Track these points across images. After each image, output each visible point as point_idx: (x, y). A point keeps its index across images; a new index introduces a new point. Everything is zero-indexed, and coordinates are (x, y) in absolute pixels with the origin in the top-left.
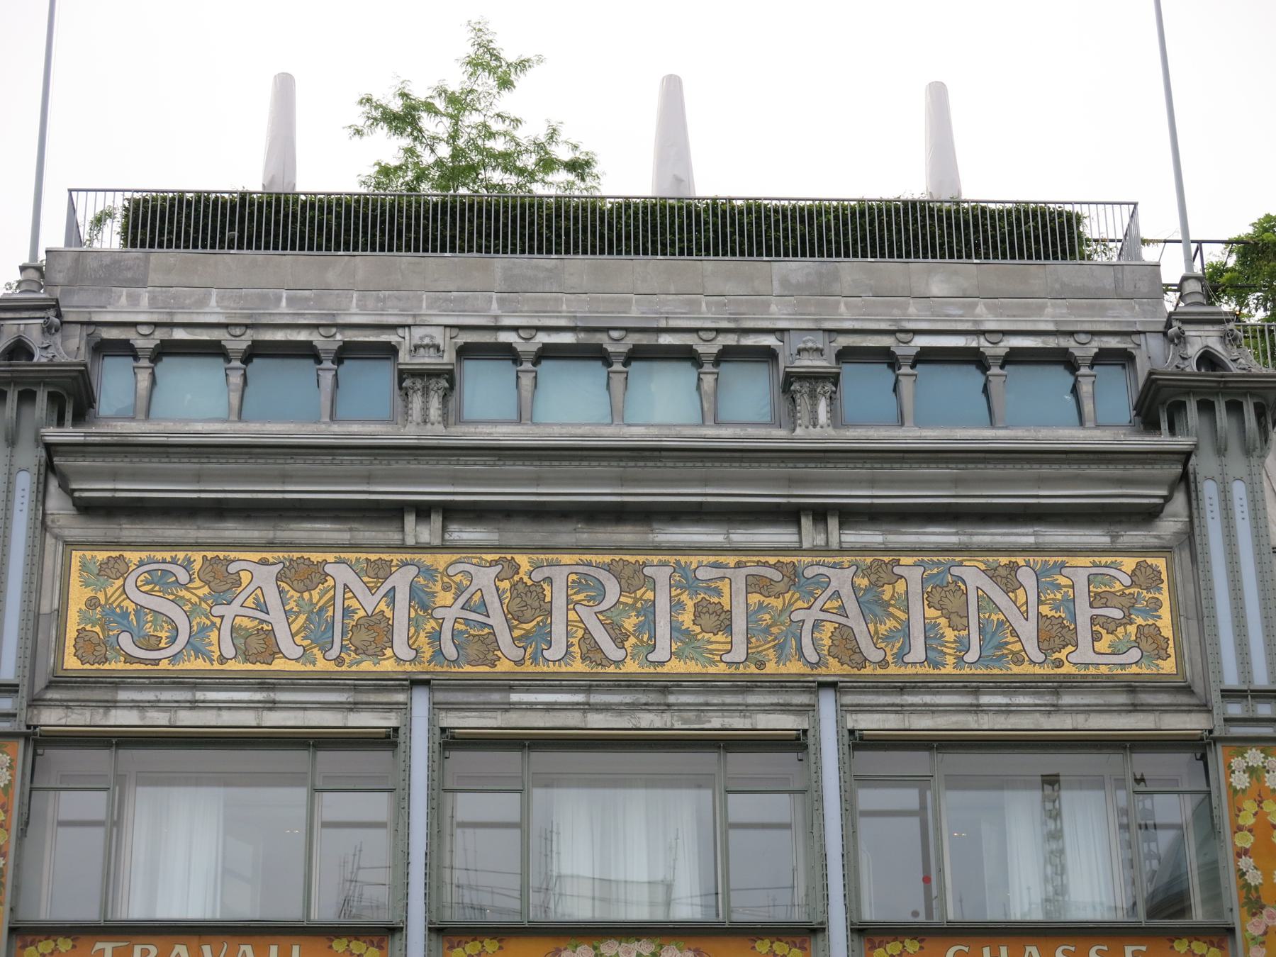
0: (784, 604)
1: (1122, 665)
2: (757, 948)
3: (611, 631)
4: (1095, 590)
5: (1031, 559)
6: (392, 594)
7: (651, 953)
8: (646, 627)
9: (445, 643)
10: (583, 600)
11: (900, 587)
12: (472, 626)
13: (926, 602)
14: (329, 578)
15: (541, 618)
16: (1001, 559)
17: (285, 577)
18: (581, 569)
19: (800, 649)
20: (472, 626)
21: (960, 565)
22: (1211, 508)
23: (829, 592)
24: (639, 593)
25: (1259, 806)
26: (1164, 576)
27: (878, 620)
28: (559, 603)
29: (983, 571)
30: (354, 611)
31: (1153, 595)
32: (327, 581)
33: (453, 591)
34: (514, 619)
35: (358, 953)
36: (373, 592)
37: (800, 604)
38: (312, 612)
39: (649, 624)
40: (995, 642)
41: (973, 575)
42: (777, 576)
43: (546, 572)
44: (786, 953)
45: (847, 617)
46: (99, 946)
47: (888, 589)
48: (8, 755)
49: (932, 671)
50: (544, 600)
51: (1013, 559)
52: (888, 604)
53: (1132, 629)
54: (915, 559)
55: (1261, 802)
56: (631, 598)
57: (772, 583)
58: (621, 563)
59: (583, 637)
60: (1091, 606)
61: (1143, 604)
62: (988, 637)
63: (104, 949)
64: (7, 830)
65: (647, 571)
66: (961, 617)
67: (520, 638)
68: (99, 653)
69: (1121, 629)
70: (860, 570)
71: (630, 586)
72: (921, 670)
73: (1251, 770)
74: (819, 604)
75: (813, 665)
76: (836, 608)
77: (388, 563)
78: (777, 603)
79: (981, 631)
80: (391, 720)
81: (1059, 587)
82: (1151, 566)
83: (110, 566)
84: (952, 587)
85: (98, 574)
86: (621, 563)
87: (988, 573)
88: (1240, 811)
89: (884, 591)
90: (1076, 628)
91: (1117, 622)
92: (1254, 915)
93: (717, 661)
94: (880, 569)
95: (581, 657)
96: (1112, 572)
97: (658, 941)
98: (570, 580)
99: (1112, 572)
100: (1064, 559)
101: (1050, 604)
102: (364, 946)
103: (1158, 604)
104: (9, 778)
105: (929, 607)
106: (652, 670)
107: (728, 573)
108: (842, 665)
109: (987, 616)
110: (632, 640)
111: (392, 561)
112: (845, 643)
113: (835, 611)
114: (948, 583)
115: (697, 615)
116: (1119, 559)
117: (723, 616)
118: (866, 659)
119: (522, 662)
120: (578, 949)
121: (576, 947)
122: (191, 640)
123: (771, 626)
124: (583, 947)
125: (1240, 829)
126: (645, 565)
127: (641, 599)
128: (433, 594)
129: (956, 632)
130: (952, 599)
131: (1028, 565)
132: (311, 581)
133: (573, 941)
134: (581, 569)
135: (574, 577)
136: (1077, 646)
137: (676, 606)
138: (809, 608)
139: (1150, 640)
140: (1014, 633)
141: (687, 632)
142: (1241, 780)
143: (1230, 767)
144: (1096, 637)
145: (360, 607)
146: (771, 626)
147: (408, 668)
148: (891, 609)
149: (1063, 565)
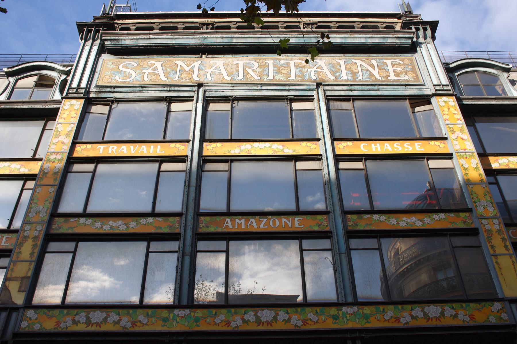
6: (194, 67)
25: (449, 109)
35: (178, 147)
41: (359, 62)
44: (311, 146)
55: (449, 109)
60: (393, 67)
65: (266, 61)
70: (326, 61)
73: (445, 102)
80: (191, 94)
88: (443, 110)
92: (453, 134)
102: (180, 146)
107: (289, 61)
117: (288, 70)
121: (246, 145)
122: (136, 77)
125: (444, 114)
139: (411, 75)
142: (442, 104)
143: (438, 101)
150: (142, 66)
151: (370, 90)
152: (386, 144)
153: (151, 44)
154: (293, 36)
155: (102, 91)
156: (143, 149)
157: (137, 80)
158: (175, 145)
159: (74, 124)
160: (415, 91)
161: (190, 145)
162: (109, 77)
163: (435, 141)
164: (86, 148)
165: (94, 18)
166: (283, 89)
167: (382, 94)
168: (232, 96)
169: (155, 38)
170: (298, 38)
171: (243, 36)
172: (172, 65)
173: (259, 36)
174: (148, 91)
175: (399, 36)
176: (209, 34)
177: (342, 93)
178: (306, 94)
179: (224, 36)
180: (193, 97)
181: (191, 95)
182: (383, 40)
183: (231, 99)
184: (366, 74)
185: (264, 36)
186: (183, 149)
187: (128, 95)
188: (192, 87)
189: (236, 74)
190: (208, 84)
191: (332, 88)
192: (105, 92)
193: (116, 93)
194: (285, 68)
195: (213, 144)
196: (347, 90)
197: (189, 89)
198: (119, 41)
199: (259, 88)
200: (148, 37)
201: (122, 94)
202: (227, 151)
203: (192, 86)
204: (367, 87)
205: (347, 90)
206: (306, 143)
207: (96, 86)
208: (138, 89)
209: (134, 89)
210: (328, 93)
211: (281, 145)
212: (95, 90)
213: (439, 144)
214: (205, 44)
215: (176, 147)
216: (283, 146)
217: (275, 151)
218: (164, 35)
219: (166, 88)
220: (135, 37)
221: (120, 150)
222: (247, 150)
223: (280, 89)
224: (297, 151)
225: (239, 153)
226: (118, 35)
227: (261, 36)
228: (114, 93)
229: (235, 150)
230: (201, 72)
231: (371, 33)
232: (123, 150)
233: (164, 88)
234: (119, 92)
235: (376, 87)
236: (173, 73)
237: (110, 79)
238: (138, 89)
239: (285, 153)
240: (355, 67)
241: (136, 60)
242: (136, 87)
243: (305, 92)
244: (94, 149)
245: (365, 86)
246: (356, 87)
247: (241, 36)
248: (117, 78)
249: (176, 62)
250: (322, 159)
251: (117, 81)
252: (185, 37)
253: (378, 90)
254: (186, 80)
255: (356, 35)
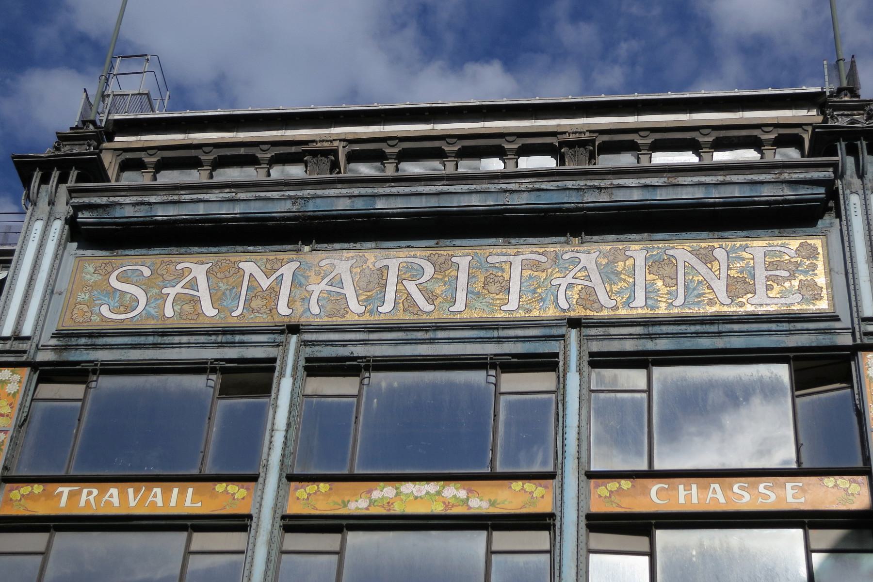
0: (547, 275)
1: (789, 305)
2: (513, 487)
3: (426, 295)
4: (769, 260)
5: (724, 244)
6: (281, 278)
7: (436, 492)
8: (450, 291)
9: (311, 307)
10: (408, 277)
11: (630, 262)
12: (332, 295)
13: (647, 271)
14: (240, 270)
15: (378, 288)
16: (701, 244)
17: (213, 271)
18: (409, 260)
19: (556, 303)
20: (332, 295)
21: (673, 248)
22: (855, 210)
23: (580, 266)
24: (447, 273)
26: (820, 250)
27: (611, 283)
28: (392, 279)
29: (689, 251)
30: (255, 288)
31: (811, 261)
32: (239, 272)
33: (322, 275)
34: (360, 289)
36: (268, 277)
37: (558, 275)
38: (227, 289)
39: (452, 290)
40: (696, 292)
42: (543, 259)
43: (386, 262)
44: (533, 490)
45: (591, 281)
46: (60, 489)
47: (621, 264)
48: (19, 375)
49: (649, 311)
50: (382, 279)
51: (711, 244)
52: (620, 273)
53: (796, 283)
54: (641, 246)
56: (441, 275)
57: (540, 263)
58: (437, 255)
59: (406, 298)
61: (804, 267)
62: (690, 291)
63: (63, 491)
64: (11, 418)
65: (454, 259)
66: (672, 279)
67: (363, 301)
68: (87, 316)
69: (787, 284)
70: (601, 255)
71: (442, 269)
72: (640, 311)
74: (572, 274)
75: (564, 311)
76: (584, 276)
77: (281, 261)
78: (544, 275)
79: (686, 287)
81: (743, 259)
82: (810, 245)
83: (102, 268)
84: (667, 262)
85: (93, 273)
86: (437, 255)
87: (693, 252)
89: (618, 265)
90: (754, 283)
91: (785, 279)
93: (497, 310)
94: (616, 253)
95: (404, 310)
96: (783, 249)
97: (442, 483)
98: (401, 266)
99: (783, 249)
100: (746, 242)
101: (736, 269)
102: (237, 488)
103: (814, 267)
104: (18, 388)
105: (650, 274)
106: (452, 316)
107: (510, 258)
108: (585, 310)
109: (691, 277)
110: (440, 299)
111: (283, 259)
112: (588, 296)
113: (583, 278)
114: (664, 259)
115: (485, 284)
116: (787, 242)
117: (504, 284)
118: (603, 306)
119: (363, 314)
120: (385, 489)
121: (383, 488)
122: (146, 308)
123: (537, 288)
124: (388, 488)
126: (453, 256)
127: (448, 276)
128: (308, 277)
129: (668, 289)
130: (666, 268)
131: (721, 247)
132: (229, 272)
133: (382, 484)
134: (409, 260)
135: (405, 264)
136: (755, 293)
137: (470, 277)
138: (565, 277)
140: (710, 287)
141: (478, 294)
144: (769, 288)
145: (259, 285)
146: (537, 288)
147: (286, 320)
148: (623, 276)
149: (747, 246)
150: (162, 275)
151: (698, 334)
152: (712, 486)
153: (184, 217)
154: (523, 187)
155: (69, 343)
156: (155, 496)
157: (149, 316)
158: (227, 486)
159: (5, 432)
160: (813, 337)
161: (259, 488)
162: (87, 307)
163: (837, 477)
164: (31, 492)
165: (58, 137)
166: (485, 336)
167: (728, 346)
168: (365, 357)
169: (192, 201)
170: (534, 193)
171: (401, 190)
172: (232, 272)
173: (439, 189)
174: (172, 346)
175: (795, 177)
176: (318, 186)
177: (629, 346)
178: (541, 351)
179: (356, 191)
180: (274, 360)
181: (271, 356)
182: (751, 190)
183: (362, 365)
184: (694, 289)
185: (452, 188)
186: (243, 498)
187: (129, 354)
188: (274, 333)
189: (379, 296)
190: (311, 325)
191: (606, 333)
192: (77, 347)
193: (101, 349)
194: (496, 279)
195: (312, 485)
196: (640, 337)
197: (266, 340)
198: (108, 209)
199: (430, 335)
200: (176, 198)
201: (115, 351)
202: (340, 502)
203: (272, 332)
204: (693, 329)
205: (640, 337)
206: (523, 484)
207: (56, 332)
208: (151, 339)
209: (142, 340)
210: (595, 347)
211: (464, 489)
212: (54, 342)
213: (847, 486)
214: (309, 213)
215: (228, 493)
216: (469, 491)
217: (449, 503)
218: (214, 191)
219: (213, 338)
220: (146, 199)
221: (104, 499)
222: (385, 502)
223: (479, 336)
224: (499, 504)
225: (367, 509)
226: (106, 194)
227: (445, 189)
228: (97, 348)
229: (359, 501)
230: (299, 293)
231: (721, 172)
232: (110, 499)
233: (210, 338)
234: (108, 347)
235: (714, 328)
236: (233, 295)
237: (87, 312)
238: (151, 339)
239: (470, 508)
240: (667, 270)
241: (149, 260)
242: (146, 334)
243: (537, 344)
244: (48, 496)
245: (688, 326)
246: (665, 329)
247: (394, 190)
248: (105, 310)
249: (241, 265)
250: (554, 525)
251: (103, 318)
252: (262, 195)
253: (719, 334)
254: (260, 315)
255: (681, 180)
